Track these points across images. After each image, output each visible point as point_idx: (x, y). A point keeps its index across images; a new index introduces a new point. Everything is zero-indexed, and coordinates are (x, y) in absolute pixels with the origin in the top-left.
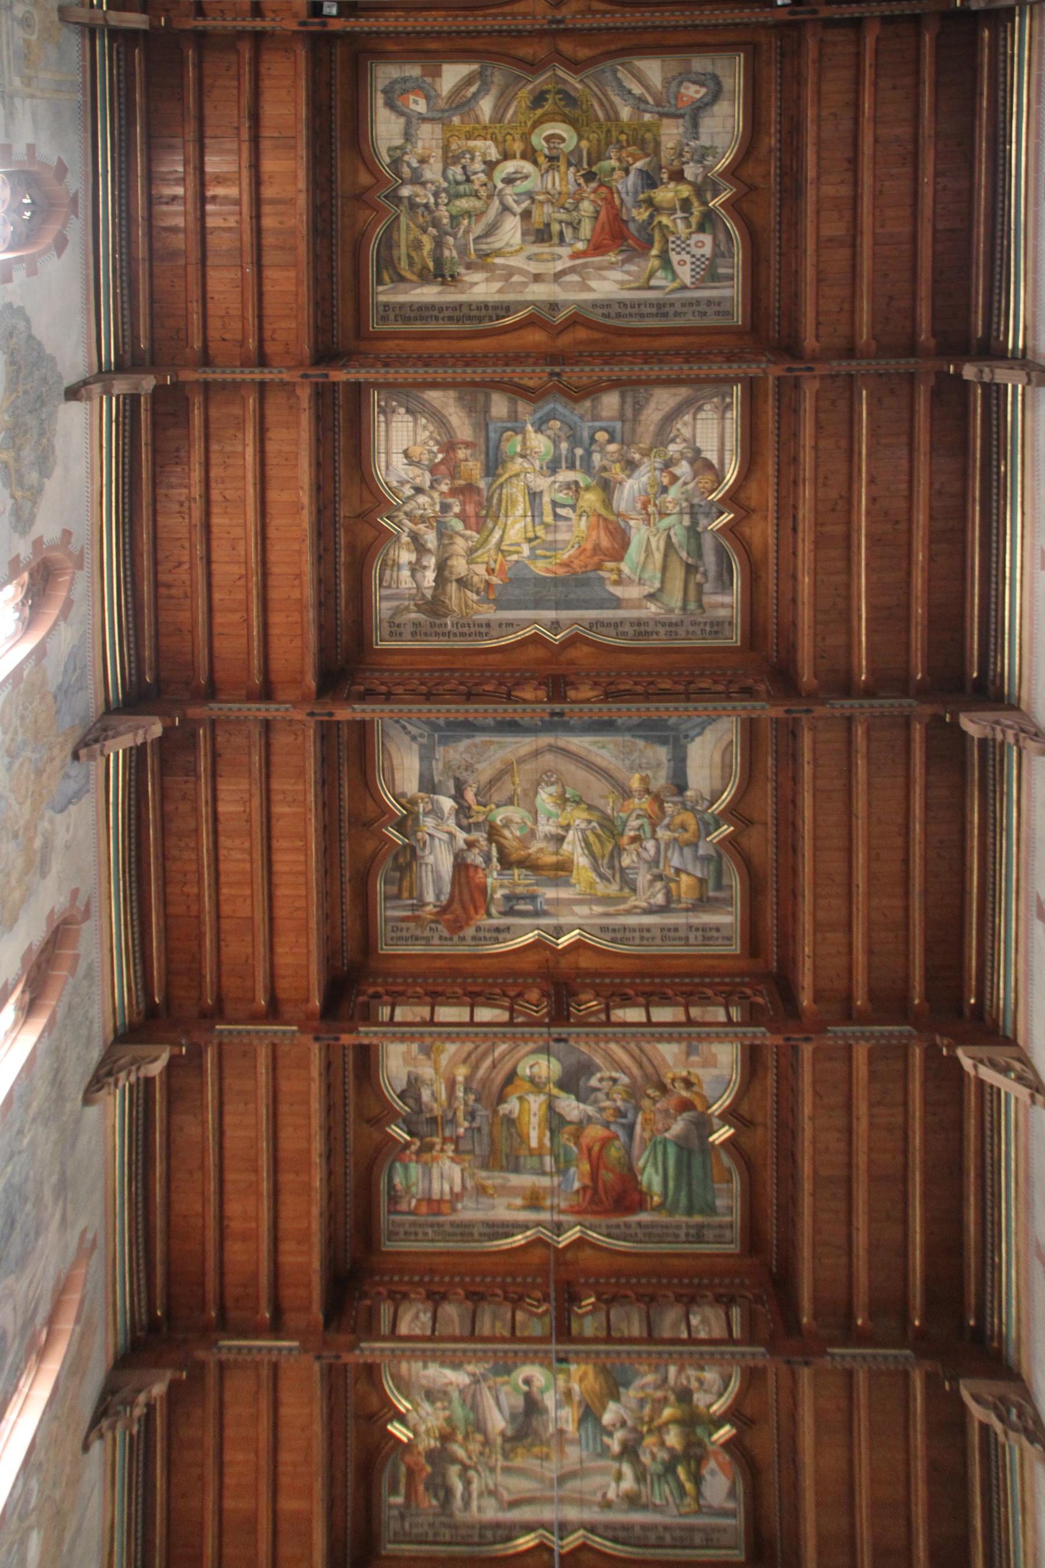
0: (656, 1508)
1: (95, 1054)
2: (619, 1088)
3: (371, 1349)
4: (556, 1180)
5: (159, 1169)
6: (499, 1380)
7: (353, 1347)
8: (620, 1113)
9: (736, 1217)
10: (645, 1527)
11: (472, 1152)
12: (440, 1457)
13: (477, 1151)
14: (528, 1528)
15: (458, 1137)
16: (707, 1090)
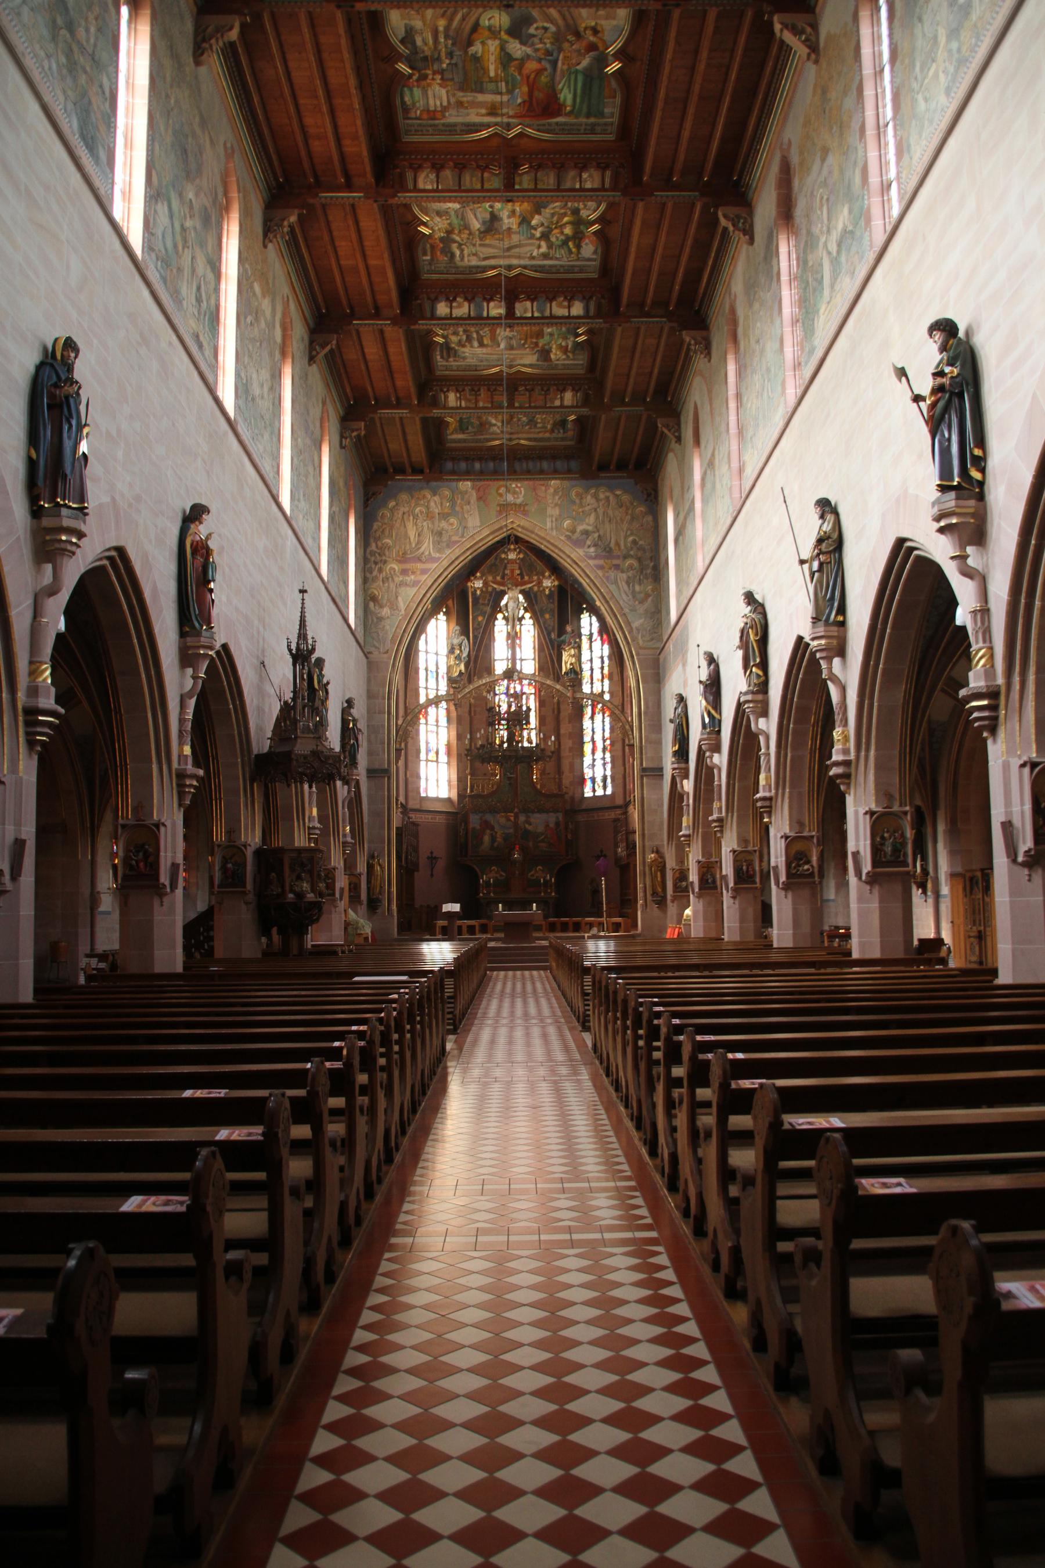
0: (557, 259)
1: (189, 26)
2: (548, 35)
3: (403, 197)
4: (505, 98)
5: (256, 100)
6: (476, 206)
7: (395, 196)
8: (548, 53)
9: (615, 119)
10: (551, 266)
11: (452, 79)
12: (447, 240)
13: (456, 80)
14: (494, 268)
15: (443, 70)
16: (607, 37)
